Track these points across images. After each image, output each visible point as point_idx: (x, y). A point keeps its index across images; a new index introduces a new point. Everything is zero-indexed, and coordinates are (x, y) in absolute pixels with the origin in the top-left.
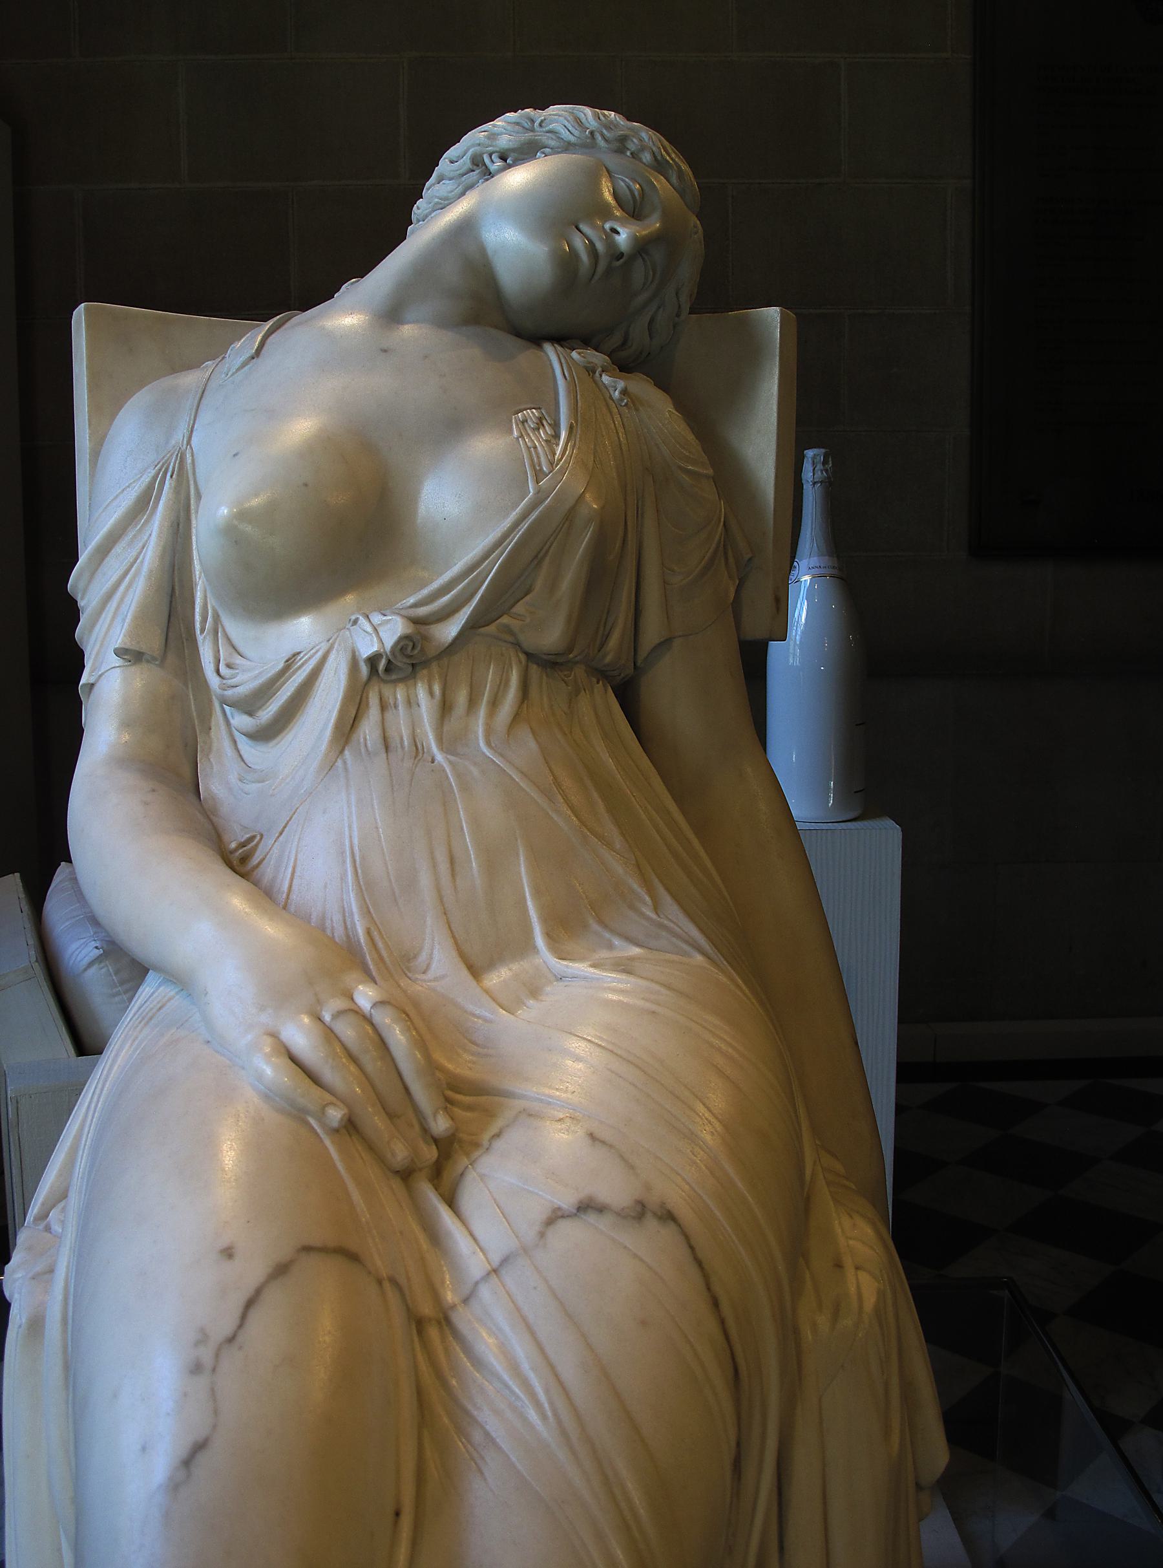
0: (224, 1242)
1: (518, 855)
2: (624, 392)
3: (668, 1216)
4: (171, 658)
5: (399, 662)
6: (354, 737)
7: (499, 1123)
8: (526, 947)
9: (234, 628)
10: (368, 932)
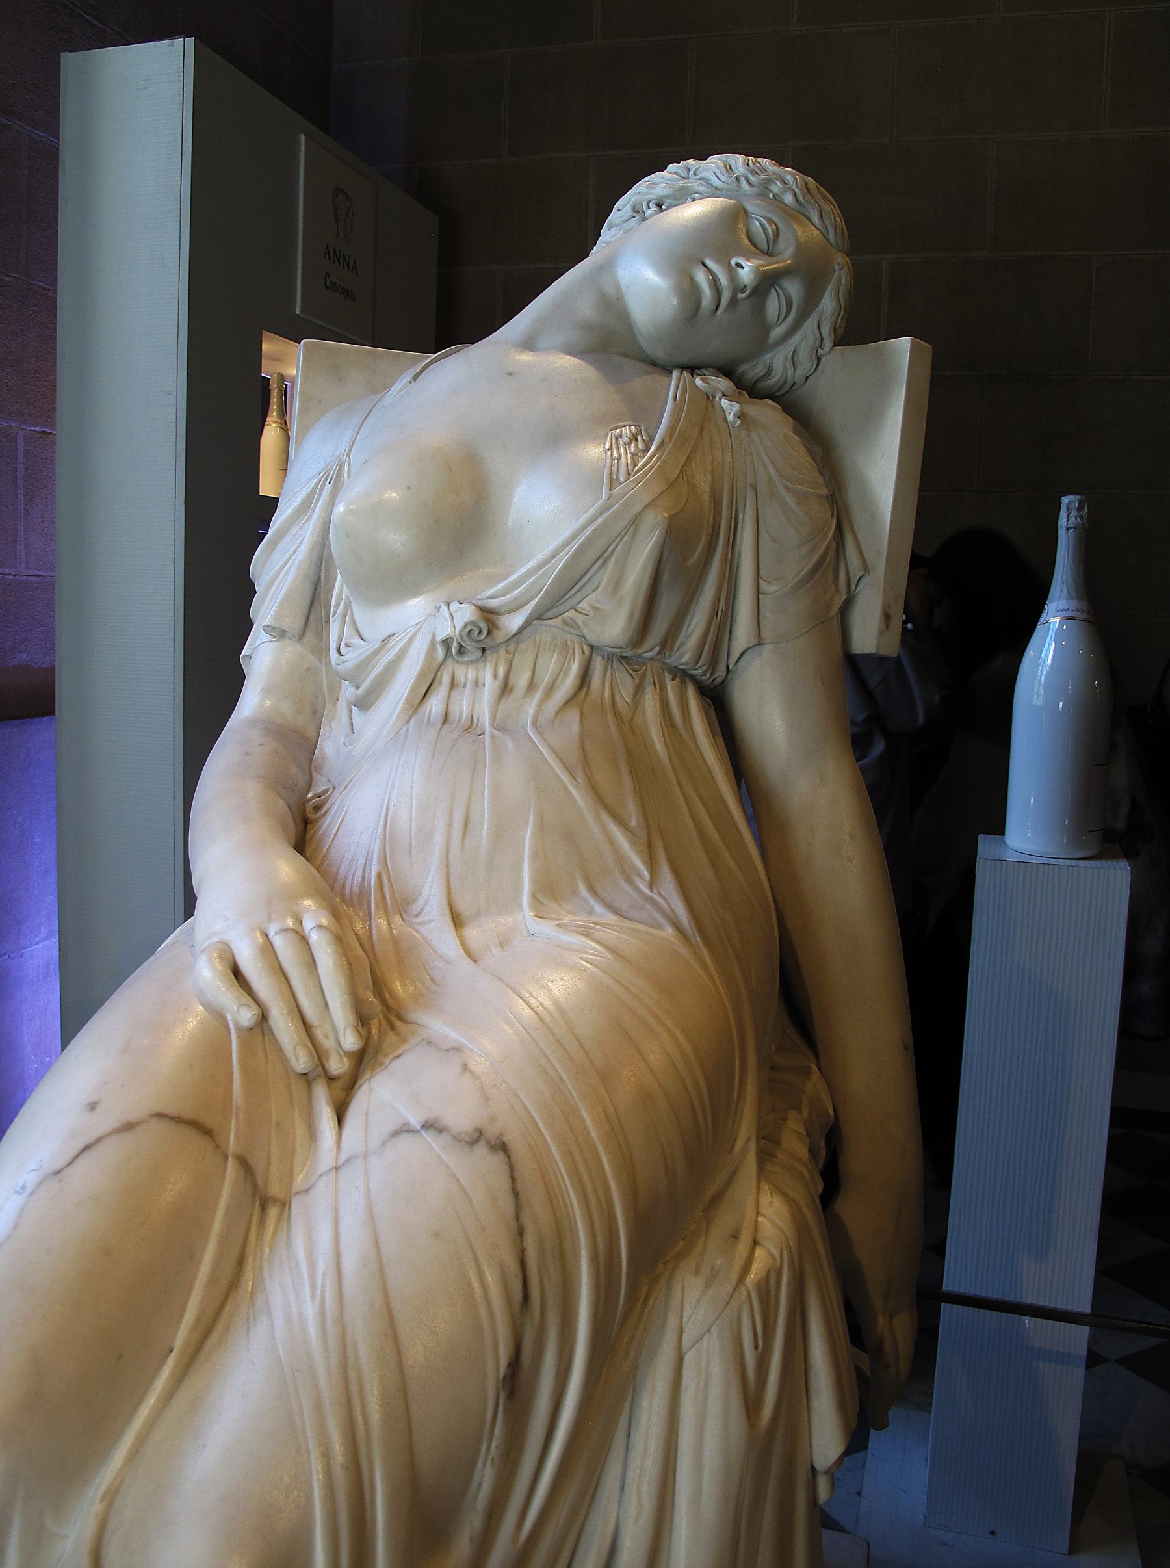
0: (93, 1099)
1: (527, 822)
2: (741, 416)
3: (501, 1147)
4: (309, 635)
5: (468, 645)
6: (422, 710)
7: (406, 1046)
8: (513, 904)
9: (360, 613)
10: (379, 876)
